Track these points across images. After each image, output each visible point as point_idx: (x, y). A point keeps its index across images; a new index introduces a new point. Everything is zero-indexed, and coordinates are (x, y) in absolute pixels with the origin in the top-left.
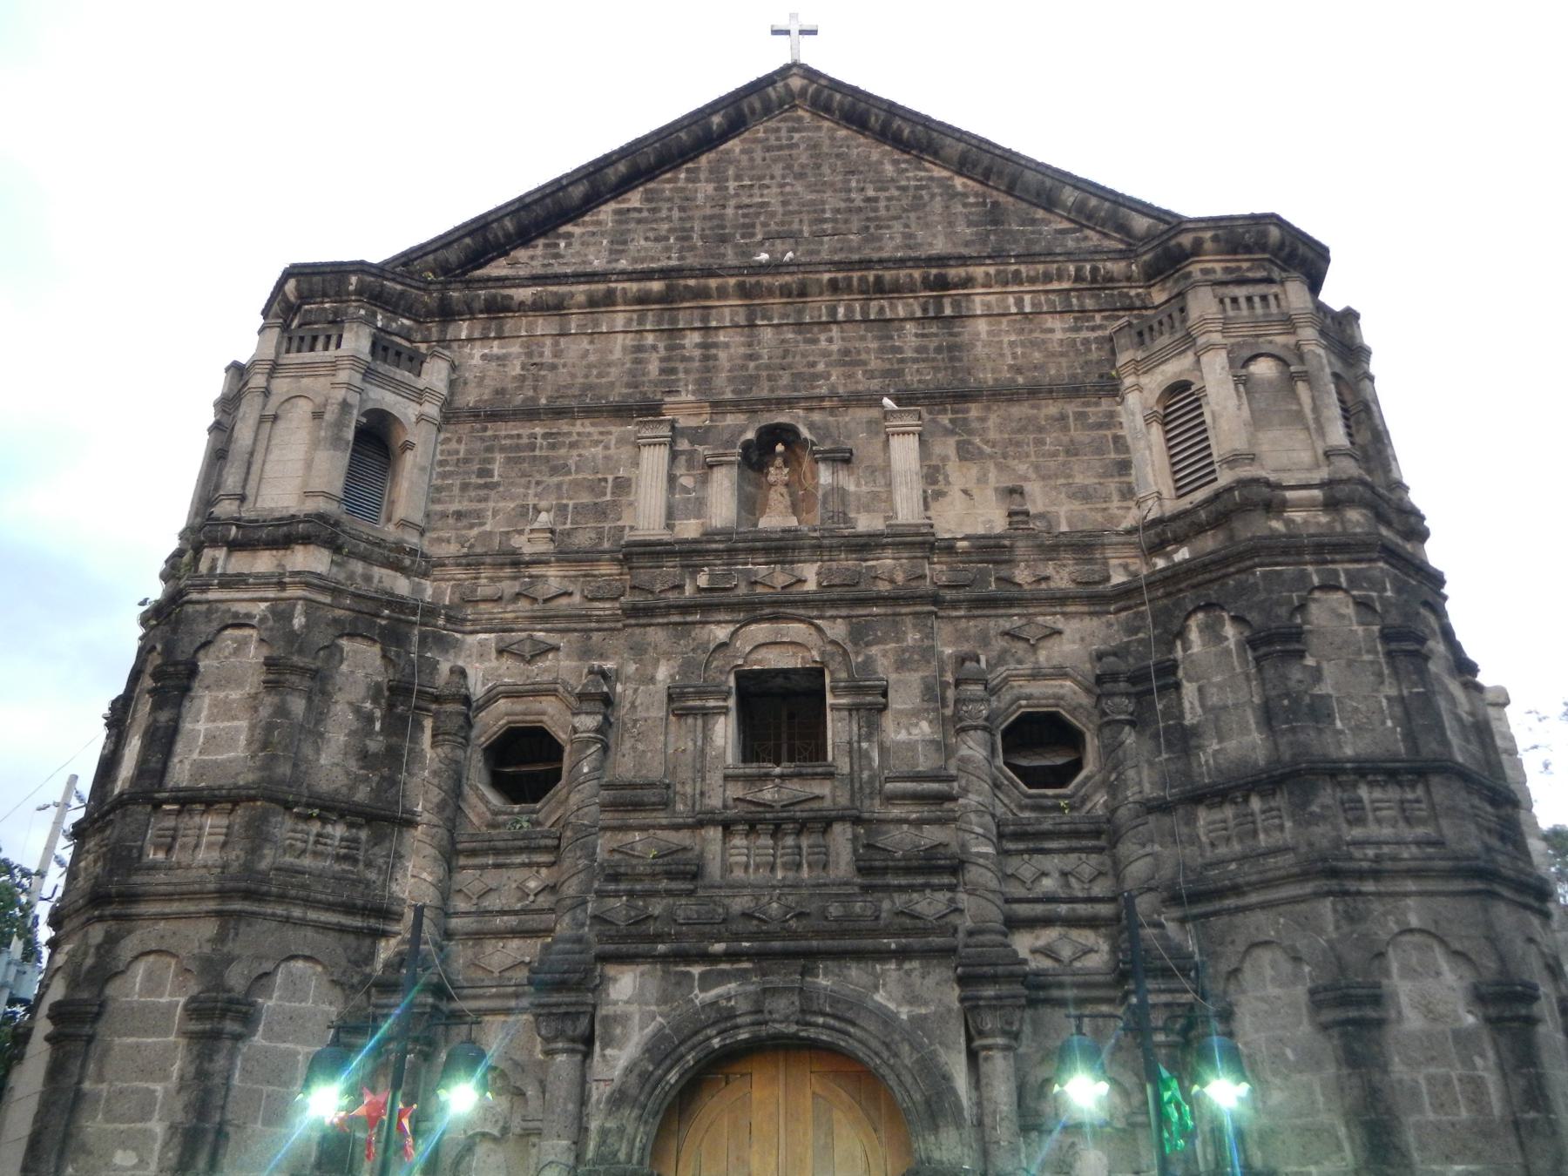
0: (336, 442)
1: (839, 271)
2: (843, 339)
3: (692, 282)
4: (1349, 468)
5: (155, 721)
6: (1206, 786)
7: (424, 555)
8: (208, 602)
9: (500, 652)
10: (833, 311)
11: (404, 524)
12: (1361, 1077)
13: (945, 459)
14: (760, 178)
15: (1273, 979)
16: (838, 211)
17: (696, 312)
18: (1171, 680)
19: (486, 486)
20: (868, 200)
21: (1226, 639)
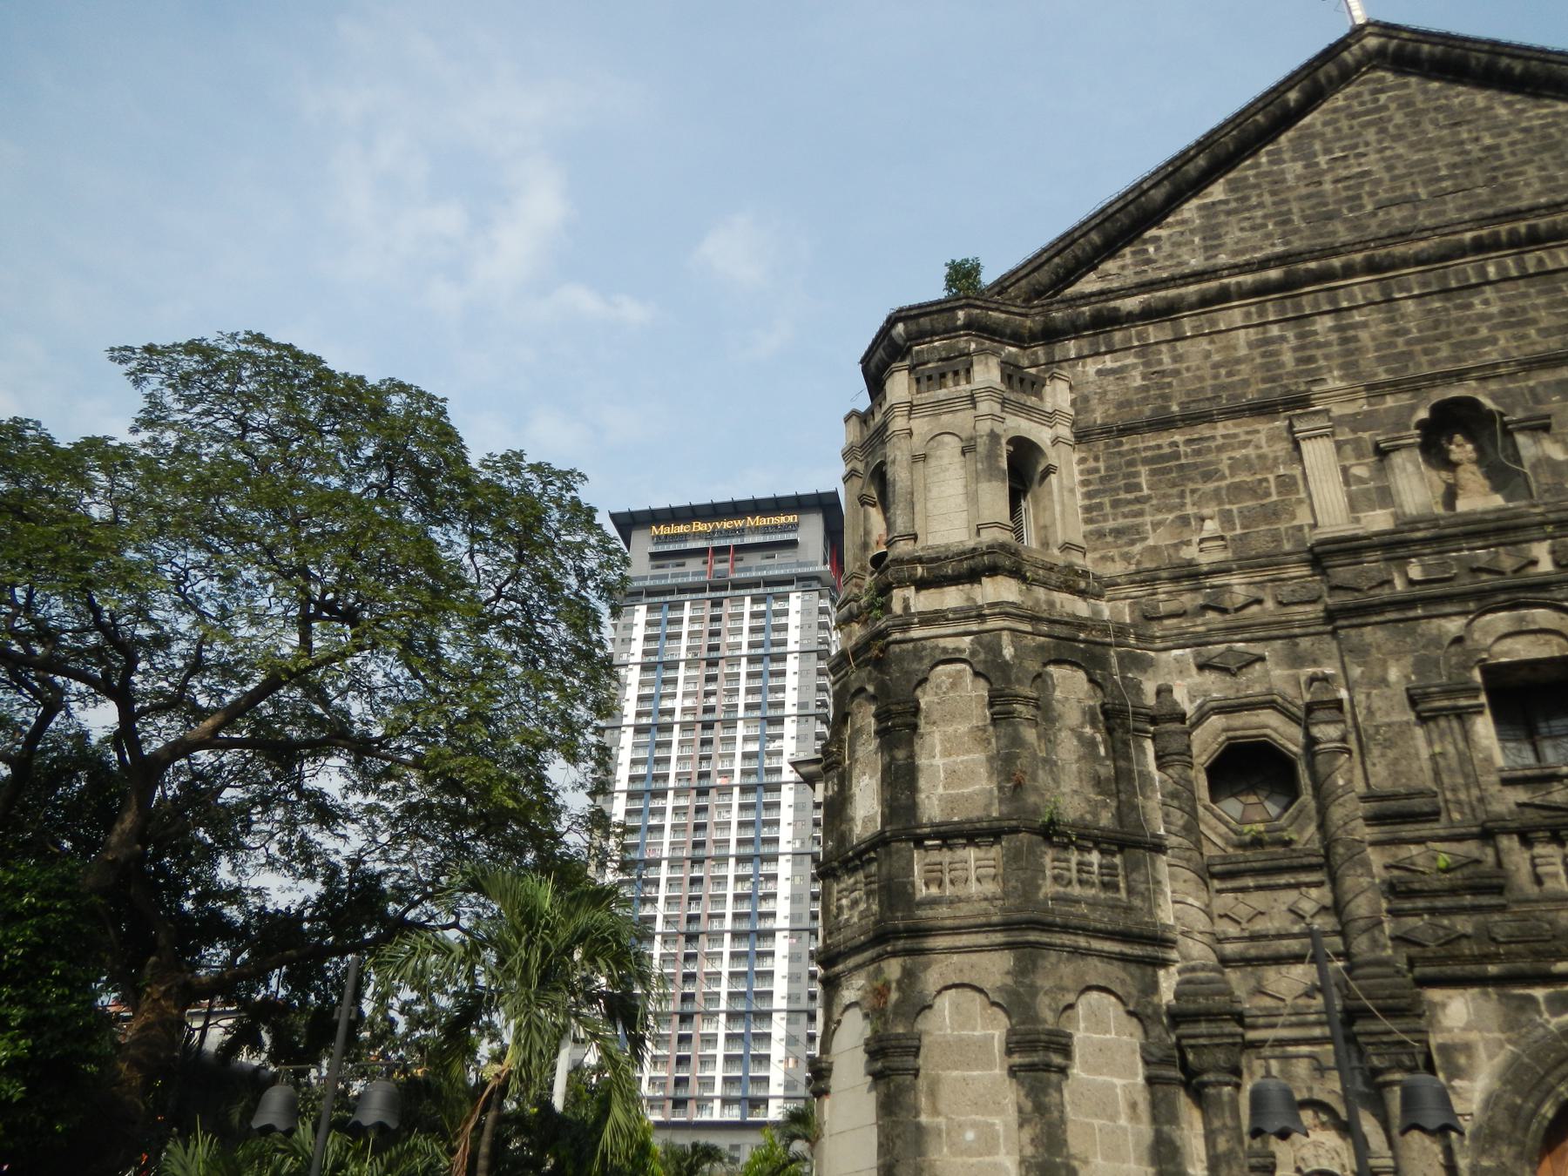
0: (992, 472)
1: (1481, 228)
2: (1502, 299)
3: (1313, 265)
5: (893, 758)
7: (1097, 578)
8: (912, 640)
10: (1482, 271)
11: (1067, 547)
14: (1356, 146)
16: (1455, 166)
17: (1321, 295)
19: (1138, 500)
20: (1488, 148)
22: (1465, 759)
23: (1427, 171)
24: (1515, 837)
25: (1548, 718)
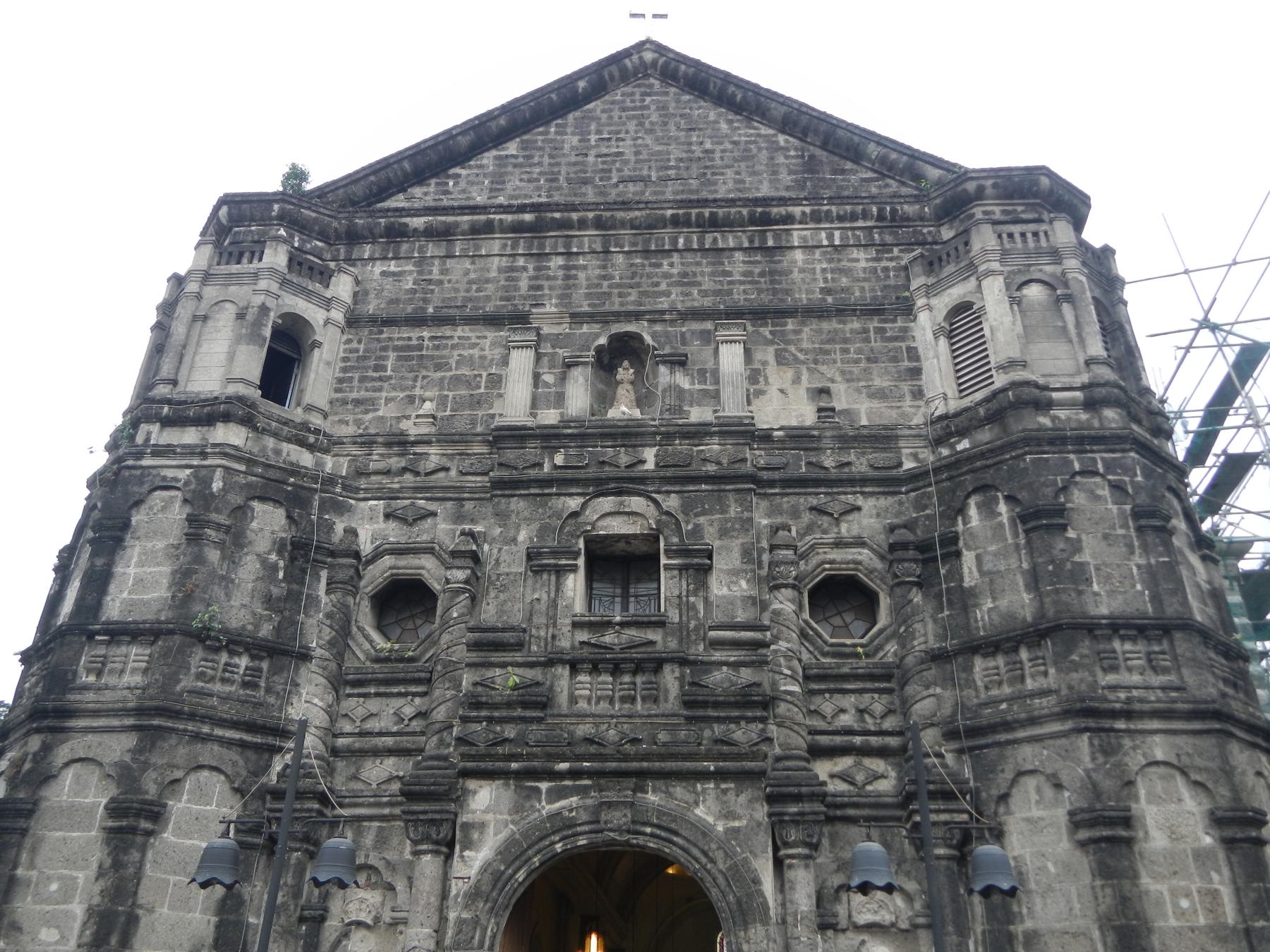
0: (254, 336)
2: (682, 264)
3: (557, 215)
4: (1106, 373)
6: (983, 637)
8: (142, 467)
9: (387, 516)
10: (674, 241)
11: (310, 408)
12: (1113, 886)
13: (765, 363)
14: (619, 132)
15: (1038, 802)
16: (681, 160)
17: (560, 240)
18: (953, 548)
19: (380, 379)
20: (707, 151)
21: (1000, 514)
22: (554, 604)
23: (662, 160)
24: (568, 667)
25: (639, 580)
